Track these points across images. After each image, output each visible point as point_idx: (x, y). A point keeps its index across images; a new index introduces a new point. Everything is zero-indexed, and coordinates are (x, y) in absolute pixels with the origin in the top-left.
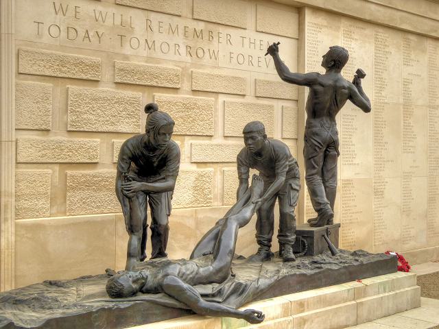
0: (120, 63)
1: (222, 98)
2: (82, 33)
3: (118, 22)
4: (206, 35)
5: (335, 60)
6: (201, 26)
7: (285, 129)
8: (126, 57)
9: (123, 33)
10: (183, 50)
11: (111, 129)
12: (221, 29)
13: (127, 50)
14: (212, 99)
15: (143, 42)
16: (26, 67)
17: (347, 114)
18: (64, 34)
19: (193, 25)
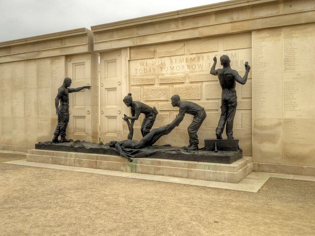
0: (160, 77)
1: (205, 84)
2: (148, 70)
3: (160, 63)
4: (196, 59)
5: (226, 62)
6: (194, 56)
7: (208, 96)
8: (163, 75)
9: (162, 67)
10: (186, 67)
11: (158, 99)
12: (204, 55)
13: (164, 72)
14: (199, 84)
15: (169, 68)
16: (132, 83)
17: (238, 86)
18: (143, 71)
19: (189, 57)
